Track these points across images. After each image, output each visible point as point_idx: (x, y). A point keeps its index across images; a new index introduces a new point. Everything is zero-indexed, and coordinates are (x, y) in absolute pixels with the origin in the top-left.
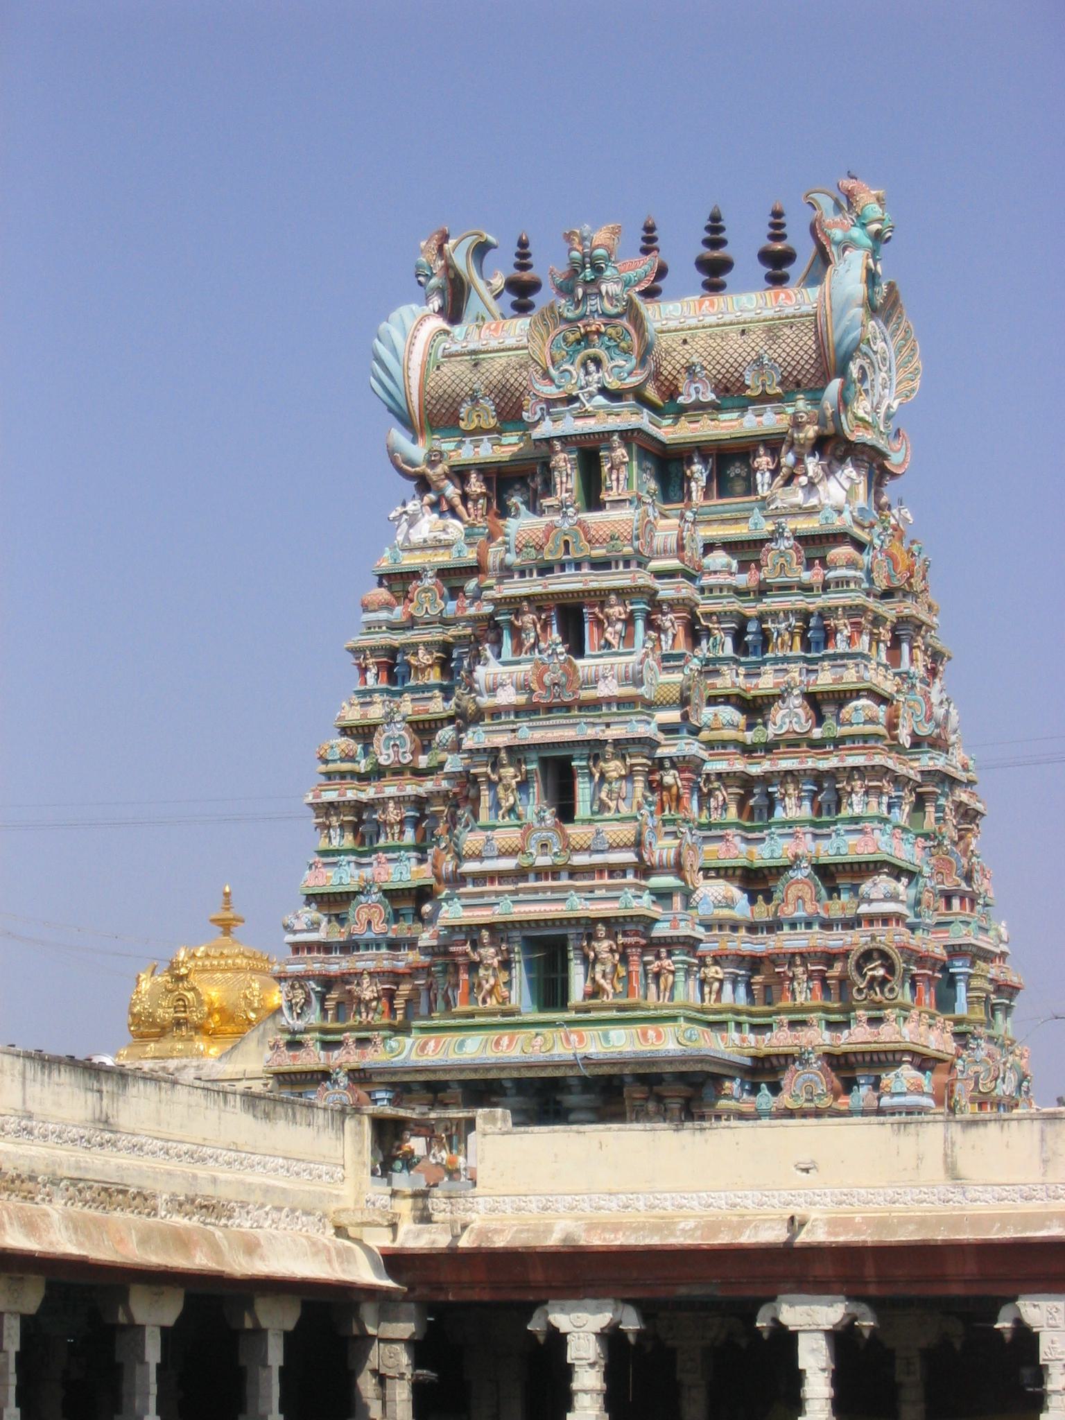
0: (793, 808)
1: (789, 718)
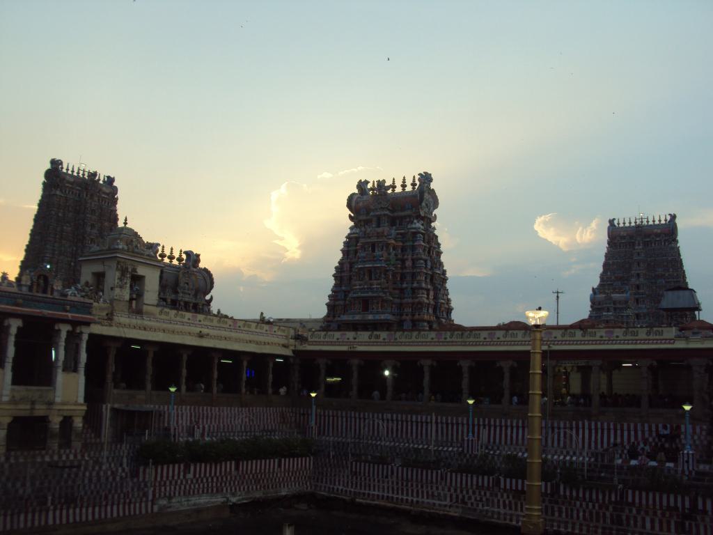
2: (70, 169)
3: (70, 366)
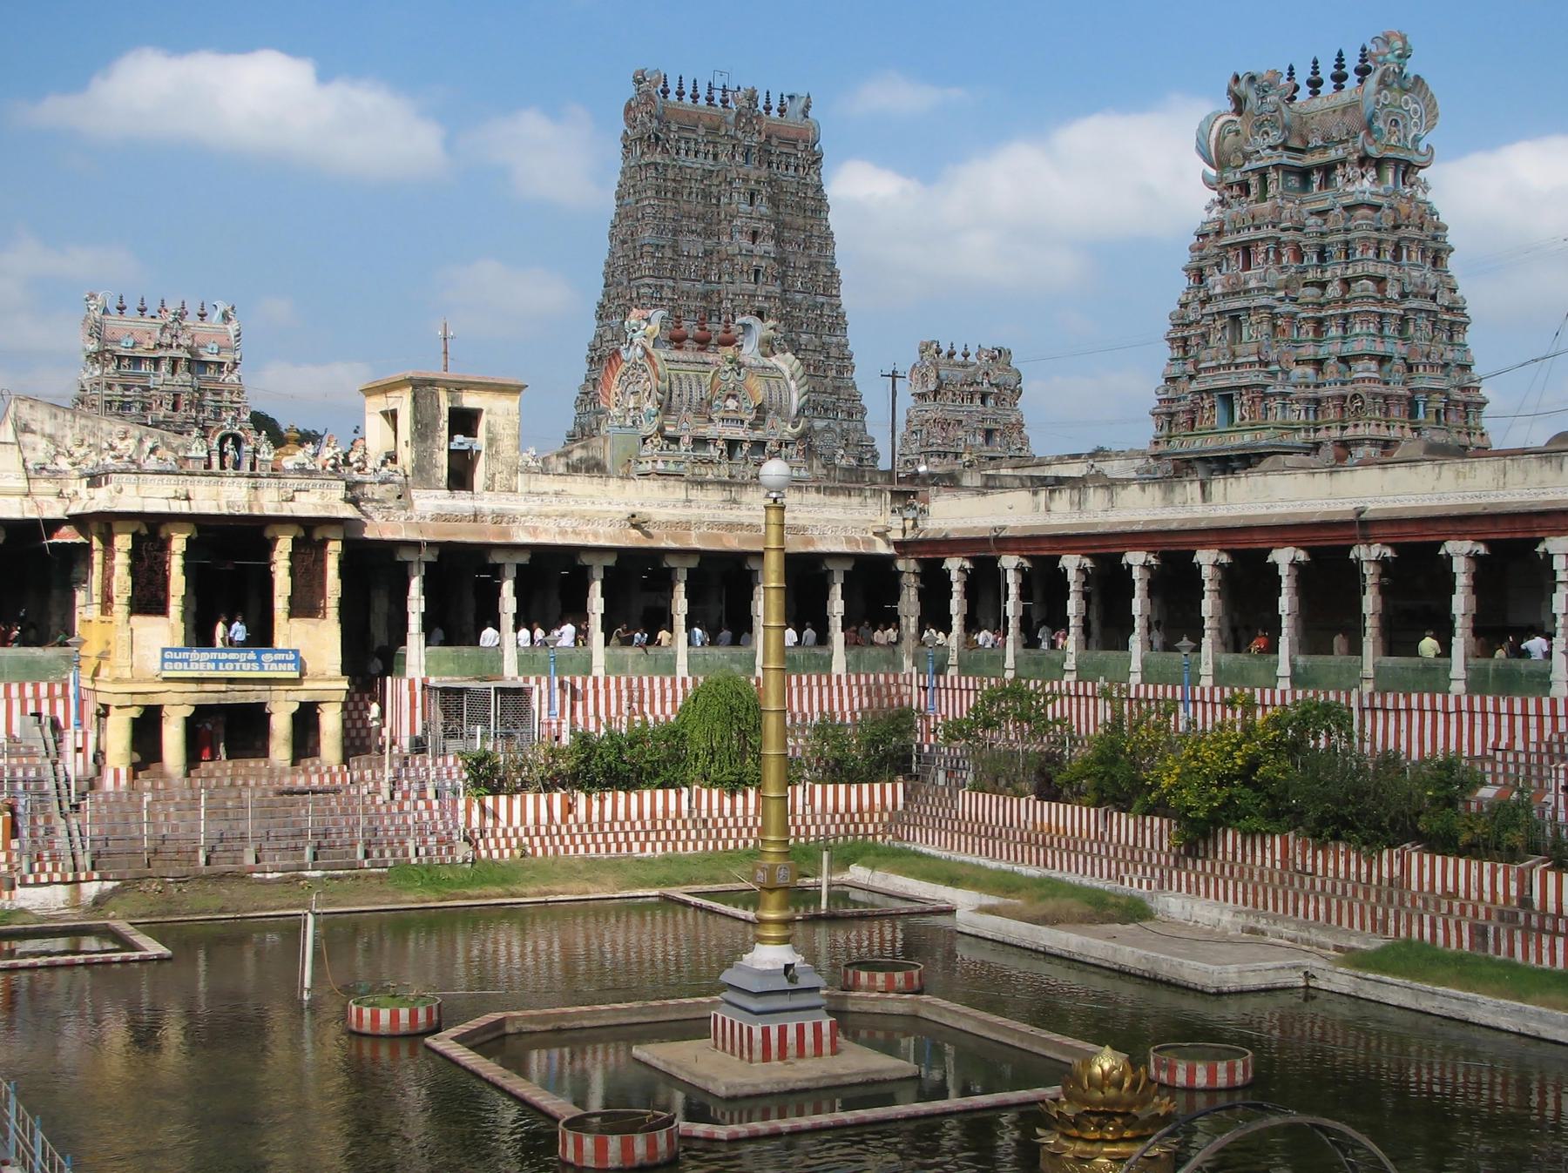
0: (1334, 332)
1: (1334, 291)
2: (688, 90)
3: (305, 604)
